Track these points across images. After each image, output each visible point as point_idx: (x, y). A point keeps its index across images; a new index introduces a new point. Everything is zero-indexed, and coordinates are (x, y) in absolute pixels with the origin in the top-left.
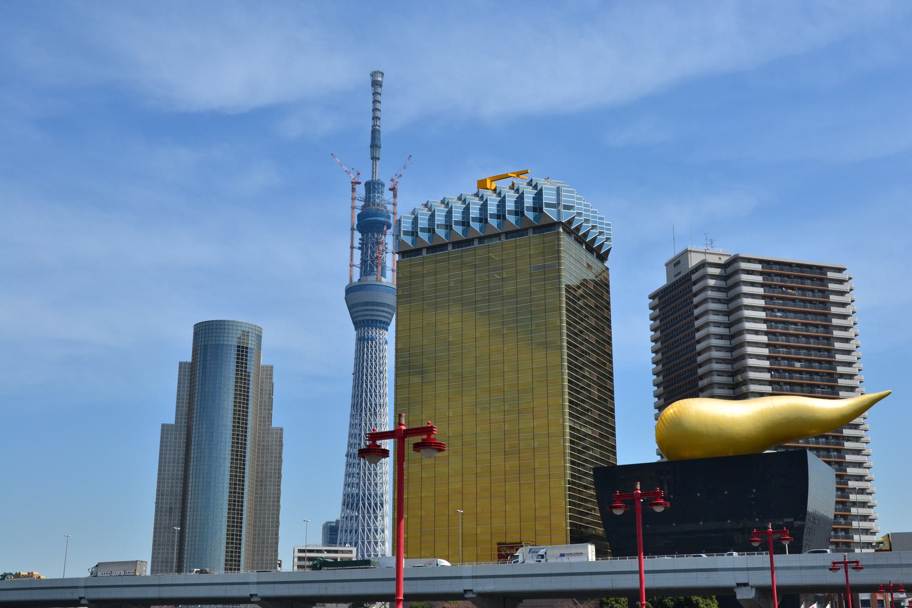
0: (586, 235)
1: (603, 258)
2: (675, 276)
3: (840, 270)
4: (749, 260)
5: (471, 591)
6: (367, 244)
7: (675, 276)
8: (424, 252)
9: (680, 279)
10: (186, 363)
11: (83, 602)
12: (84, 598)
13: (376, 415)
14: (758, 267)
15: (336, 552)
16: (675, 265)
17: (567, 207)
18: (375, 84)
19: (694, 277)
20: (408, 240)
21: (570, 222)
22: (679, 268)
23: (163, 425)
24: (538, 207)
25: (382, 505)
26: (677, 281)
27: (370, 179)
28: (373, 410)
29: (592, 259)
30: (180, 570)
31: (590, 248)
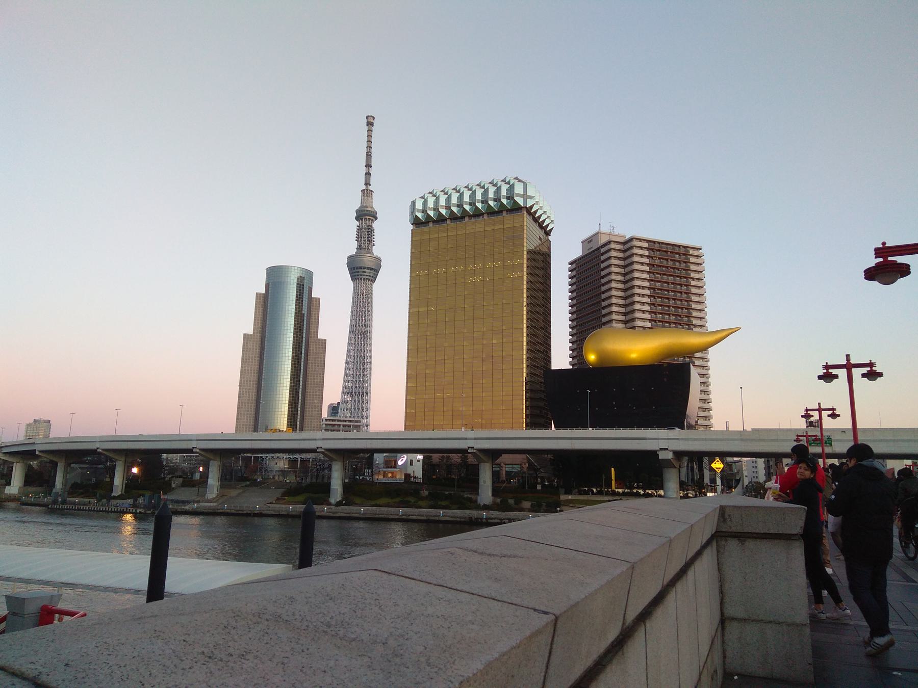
0: (540, 217)
1: (548, 233)
2: (588, 250)
3: (698, 249)
4: (640, 240)
5: (473, 448)
6: (361, 229)
7: (588, 250)
8: (431, 224)
9: (592, 252)
10: (260, 294)
11: (194, 450)
12: (196, 448)
13: (365, 338)
14: (646, 245)
15: (350, 421)
16: (589, 242)
17: (531, 197)
18: (370, 124)
19: (603, 250)
20: (420, 215)
21: (531, 207)
22: (591, 245)
23: (244, 335)
24: (510, 197)
25: (367, 393)
26: (590, 253)
27: (364, 187)
29: (541, 233)
30: (256, 430)
31: (541, 225)
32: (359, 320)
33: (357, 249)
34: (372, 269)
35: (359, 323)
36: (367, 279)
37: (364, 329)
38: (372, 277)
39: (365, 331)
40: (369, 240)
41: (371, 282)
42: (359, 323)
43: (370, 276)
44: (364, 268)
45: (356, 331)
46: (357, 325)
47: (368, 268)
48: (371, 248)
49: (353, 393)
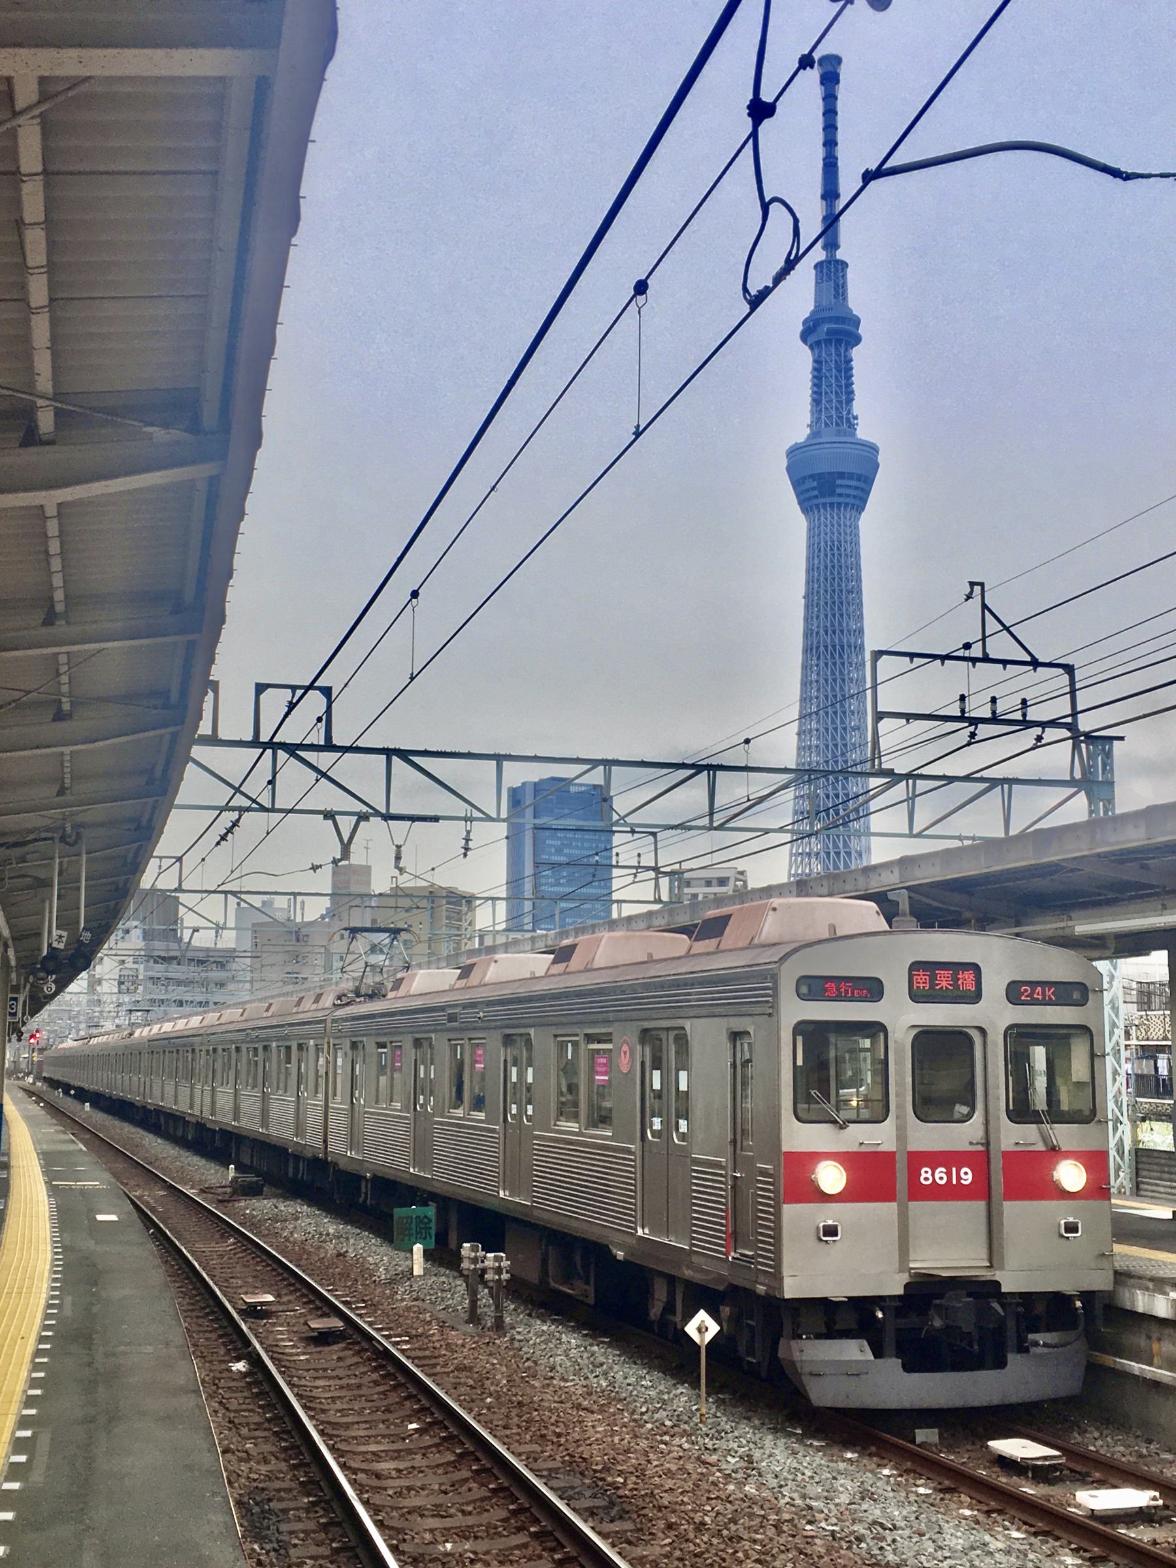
36: (839, 504)
37: (840, 640)
38: (855, 497)
39: (842, 647)
41: (854, 513)
45: (818, 648)
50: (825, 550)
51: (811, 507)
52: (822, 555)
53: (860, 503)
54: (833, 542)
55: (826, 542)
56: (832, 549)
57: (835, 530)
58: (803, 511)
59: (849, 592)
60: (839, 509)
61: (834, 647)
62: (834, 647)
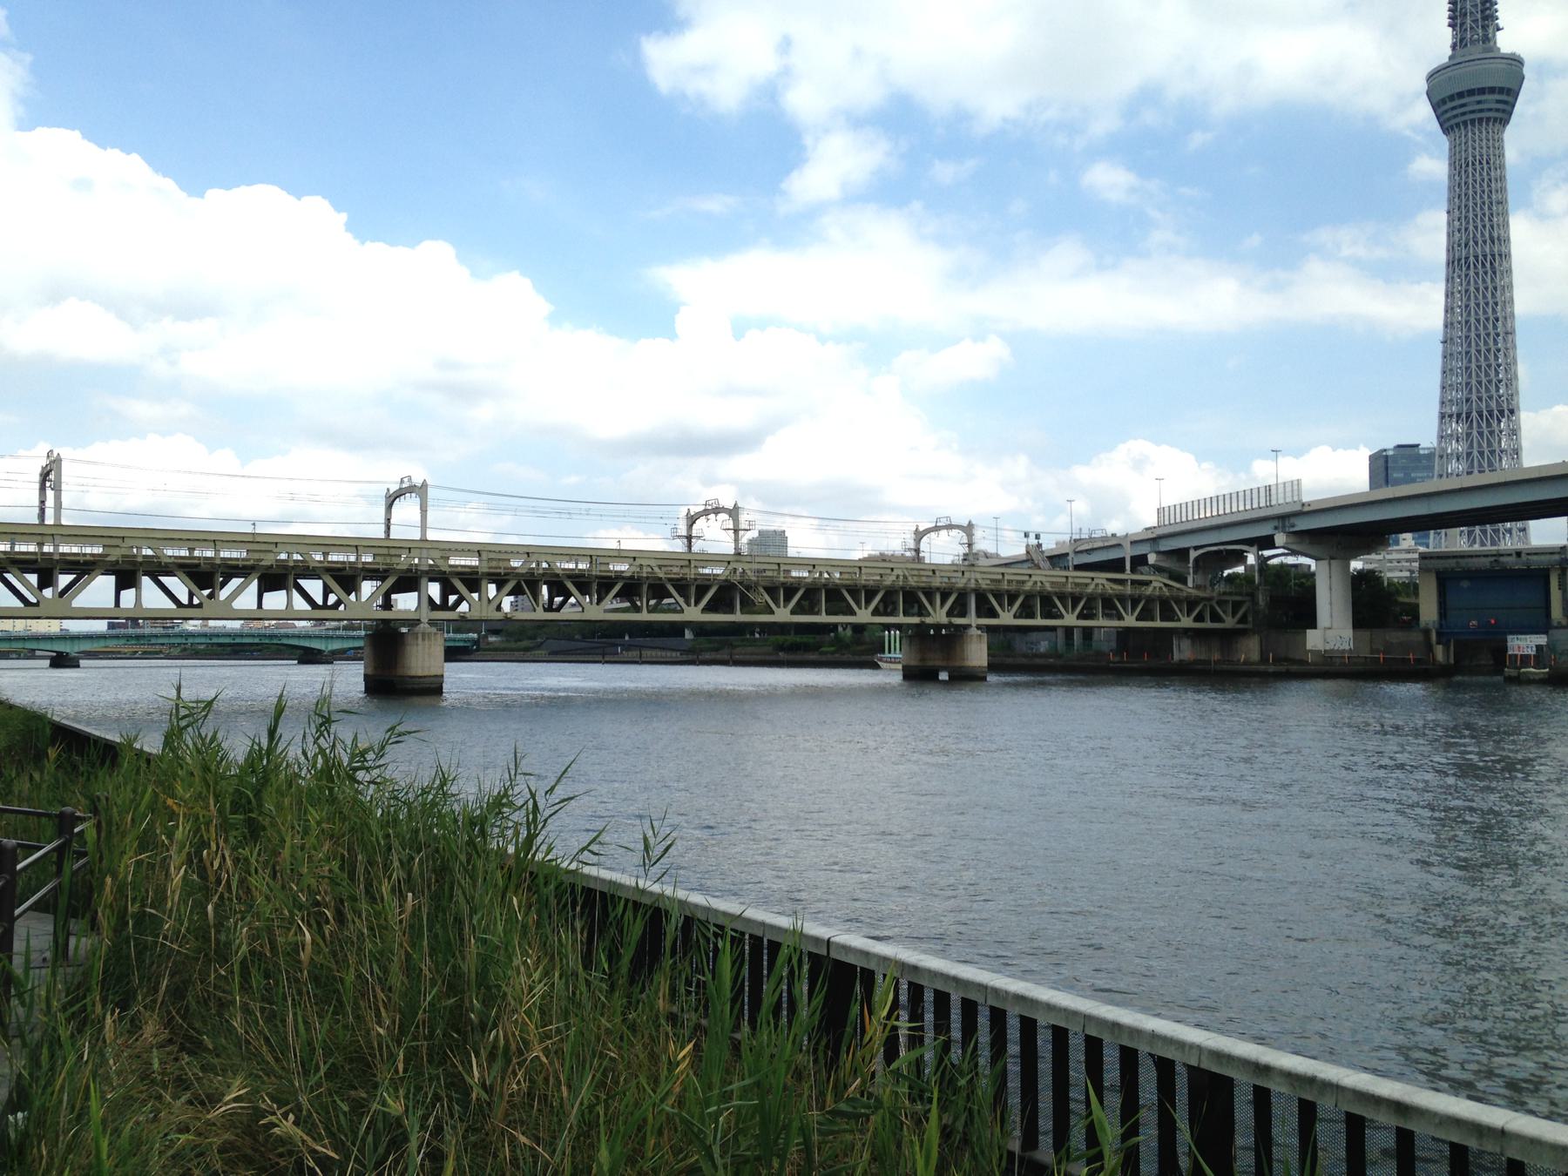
25: (1512, 412)
28: (1488, 265)
32: (1476, 228)
33: (1454, 47)
34: (1501, 90)
35: (1475, 236)
36: (1488, 119)
37: (1491, 250)
40: (1485, 18)
42: (1475, 236)
43: (1497, 110)
44: (1482, 91)
45: (1467, 258)
46: (1471, 243)
47: (1492, 90)
48: (1494, 36)
49: (1474, 414)
50: (1473, 164)
51: (1458, 125)
52: (1470, 169)
53: (1503, 115)
54: (1481, 155)
55: (1474, 157)
56: (1480, 163)
57: (1477, 145)
58: (1444, 132)
59: (1499, 203)
60: (1487, 124)
61: (1485, 256)
62: (1485, 256)
